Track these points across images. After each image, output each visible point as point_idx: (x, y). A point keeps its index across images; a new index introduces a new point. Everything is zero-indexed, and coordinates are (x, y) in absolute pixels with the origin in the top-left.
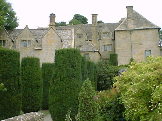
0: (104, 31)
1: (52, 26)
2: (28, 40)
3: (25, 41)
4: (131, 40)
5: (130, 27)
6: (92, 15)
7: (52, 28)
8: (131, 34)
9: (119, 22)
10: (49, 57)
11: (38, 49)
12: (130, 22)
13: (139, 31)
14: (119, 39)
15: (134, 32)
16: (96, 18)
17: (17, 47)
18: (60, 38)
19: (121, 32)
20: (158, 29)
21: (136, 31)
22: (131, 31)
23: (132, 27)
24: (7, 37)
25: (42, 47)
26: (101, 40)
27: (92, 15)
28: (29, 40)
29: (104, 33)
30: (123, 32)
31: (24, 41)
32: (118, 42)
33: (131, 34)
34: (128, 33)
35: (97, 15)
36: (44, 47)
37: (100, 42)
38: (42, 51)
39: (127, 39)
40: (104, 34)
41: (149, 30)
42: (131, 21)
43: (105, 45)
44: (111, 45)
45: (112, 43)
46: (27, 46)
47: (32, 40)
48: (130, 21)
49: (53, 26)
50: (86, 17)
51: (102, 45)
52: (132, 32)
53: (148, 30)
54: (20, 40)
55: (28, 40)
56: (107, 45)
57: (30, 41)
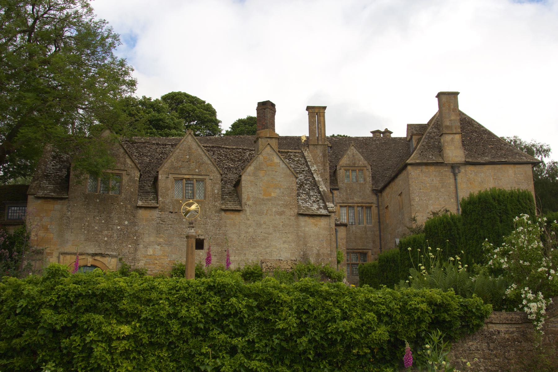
0: (348, 162)
1: (269, 140)
2: (195, 177)
3: (188, 179)
4: (457, 193)
5: (451, 155)
6: (308, 108)
7: (269, 144)
8: (455, 175)
9: (371, 135)
10: (266, 235)
11: (229, 207)
12: (452, 140)
13: (478, 167)
14: (420, 189)
15: (463, 170)
16: (322, 118)
17: (163, 198)
18: (294, 179)
19: (424, 168)
20: (530, 166)
21: (470, 168)
22: (454, 168)
23: (456, 156)
24: (125, 163)
25: (244, 201)
26: (338, 189)
27: (308, 108)
28: (200, 177)
29: (345, 170)
30: (432, 169)
31: (182, 179)
32: (417, 199)
33: (455, 175)
34: (447, 171)
35: (325, 108)
36: (248, 203)
37: (334, 196)
38: (241, 213)
39: (442, 190)
40: (347, 170)
41: (508, 167)
42: (452, 138)
43: (350, 207)
44: (370, 207)
45: (374, 199)
46: (193, 196)
47: (208, 177)
48: (451, 136)
49: (273, 139)
50: (144, 97)
51: (341, 206)
52: (457, 171)
53: (504, 166)
54: (170, 176)
55: (195, 177)
56: (355, 208)
57: (203, 180)
